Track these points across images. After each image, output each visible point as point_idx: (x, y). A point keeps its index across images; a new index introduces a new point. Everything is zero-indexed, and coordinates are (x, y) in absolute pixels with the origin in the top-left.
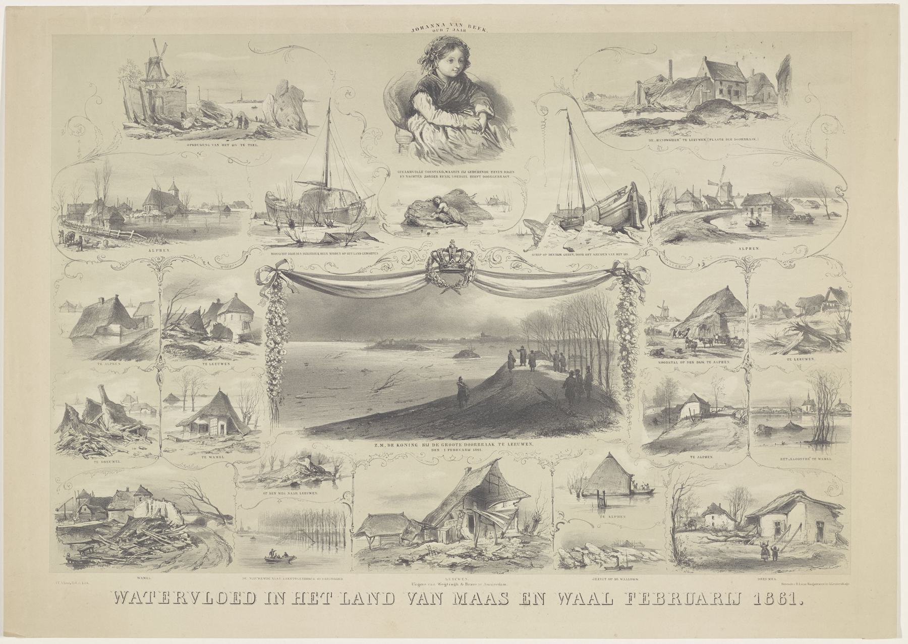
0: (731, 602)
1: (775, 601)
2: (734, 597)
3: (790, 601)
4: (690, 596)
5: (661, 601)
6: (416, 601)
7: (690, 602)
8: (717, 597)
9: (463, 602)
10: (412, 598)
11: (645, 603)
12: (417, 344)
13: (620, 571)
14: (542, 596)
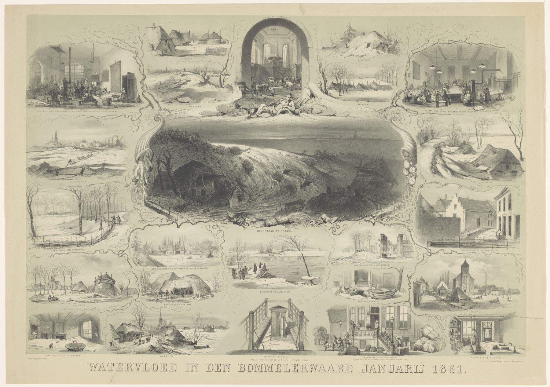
0: (418, 371)
1: (246, 369)
2: (420, 368)
3: (457, 370)
4: (392, 367)
5: (243, 370)
6: (98, 368)
7: (211, 370)
8: (331, 368)
9: (260, 370)
10: (138, 368)
11: (120, 370)
12: (62, 232)
13: (76, 352)
14: (196, 365)
